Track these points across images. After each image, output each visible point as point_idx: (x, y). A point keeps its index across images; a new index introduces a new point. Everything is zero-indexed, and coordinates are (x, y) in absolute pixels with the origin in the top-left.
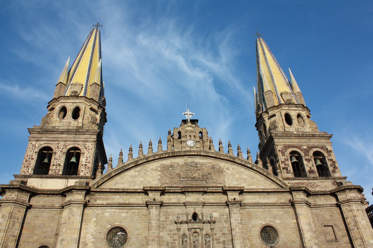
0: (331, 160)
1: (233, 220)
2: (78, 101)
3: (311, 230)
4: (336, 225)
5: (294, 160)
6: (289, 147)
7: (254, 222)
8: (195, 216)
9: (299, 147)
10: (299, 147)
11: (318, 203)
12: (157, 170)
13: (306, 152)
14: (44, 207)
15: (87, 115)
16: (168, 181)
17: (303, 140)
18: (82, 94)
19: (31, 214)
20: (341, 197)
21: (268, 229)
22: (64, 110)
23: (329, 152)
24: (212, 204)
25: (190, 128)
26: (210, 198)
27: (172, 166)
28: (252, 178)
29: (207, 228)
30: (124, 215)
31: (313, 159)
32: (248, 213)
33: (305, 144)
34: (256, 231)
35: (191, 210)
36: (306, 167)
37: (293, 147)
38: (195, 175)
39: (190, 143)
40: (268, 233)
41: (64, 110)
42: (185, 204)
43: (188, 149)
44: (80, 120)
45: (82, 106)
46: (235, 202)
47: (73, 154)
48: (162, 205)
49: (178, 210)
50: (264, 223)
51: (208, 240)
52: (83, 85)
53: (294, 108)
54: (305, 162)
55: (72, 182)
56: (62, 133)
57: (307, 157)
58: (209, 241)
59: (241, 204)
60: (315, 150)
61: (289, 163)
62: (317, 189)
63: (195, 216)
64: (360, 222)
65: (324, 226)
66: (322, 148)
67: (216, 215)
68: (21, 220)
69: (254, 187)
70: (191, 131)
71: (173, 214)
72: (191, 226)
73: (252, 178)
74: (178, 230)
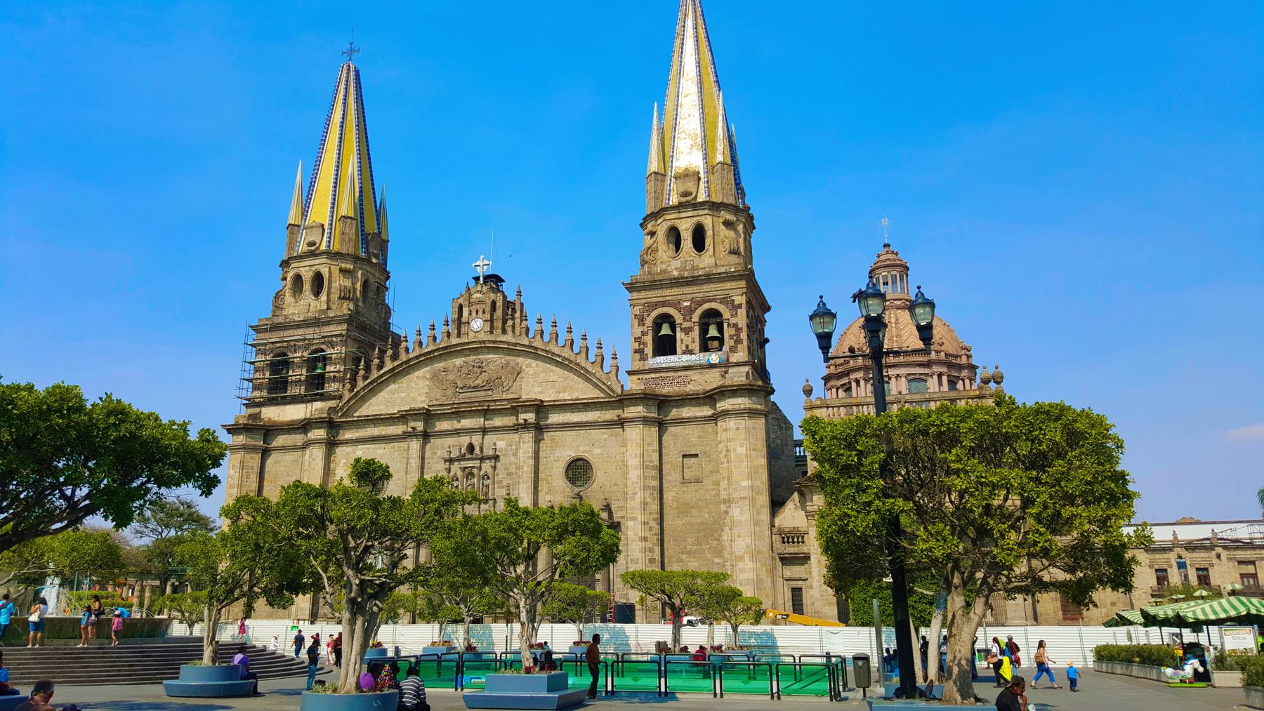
0: (735, 325)
1: (521, 454)
2: (317, 262)
3: (644, 466)
4: (705, 453)
5: (665, 330)
6: (656, 305)
7: (558, 453)
8: (471, 448)
9: (676, 305)
10: (676, 305)
11: (684, 415)
12: (424, 377)
13: (688, 313)
14: (284, 448)
15: (335, 285)
16: (438, 395)
17: (687, 290)
18: (323, 247)
19: (270, 462)
20: (723, 405)
21: (580, 463)
22: (298, 279)
23: (735, 307)
24: (496, 430)
25: (478, 295)
26: (498, 421)
27: (445, 370)
28: (565, 379)
29: (487, 466)
30: (381, 452)
31: (697, 328)
32: (553, 439)
33: (685, 295)
34: (560, 467)
35: (465, 440)
36: (678, 345)
37: (663, 304)
38: (477, 382)
39: (477, 324)
40: (578, 470)
41: (298, 279)
42: (458, 433)
43: (472, 337)
44: (323, 297)
45: (325, 271)
46: (525, 426)
47: (317, 359)
48: (426, 436)
49: (449, 441)
50: (573, 454)
51: (486, 482)
52: (323, 226)
53: (690, 214)
54: (679, 335)
55: (317, 408)
56: (298, 327)
57: (686, 325)
58: (487, 486)
59: (539, 429)
60: (706, 306)
61: (649, 339)
62: (690, 388)
63: (471, 448)
64: (735, 450)
65: (684, 456)
66: (726, 300)
67: (501, 445)
68: (256, 470)
69: (566, 396)
70: (481, 302)
71: (443, 448)
72: (464, 464)
73: (565, 379)
74: (449, 470)
